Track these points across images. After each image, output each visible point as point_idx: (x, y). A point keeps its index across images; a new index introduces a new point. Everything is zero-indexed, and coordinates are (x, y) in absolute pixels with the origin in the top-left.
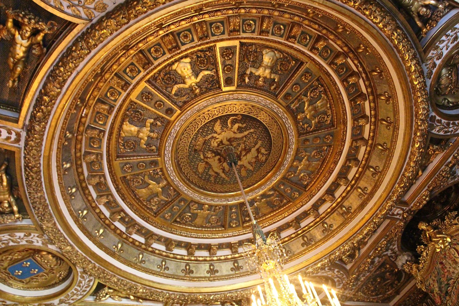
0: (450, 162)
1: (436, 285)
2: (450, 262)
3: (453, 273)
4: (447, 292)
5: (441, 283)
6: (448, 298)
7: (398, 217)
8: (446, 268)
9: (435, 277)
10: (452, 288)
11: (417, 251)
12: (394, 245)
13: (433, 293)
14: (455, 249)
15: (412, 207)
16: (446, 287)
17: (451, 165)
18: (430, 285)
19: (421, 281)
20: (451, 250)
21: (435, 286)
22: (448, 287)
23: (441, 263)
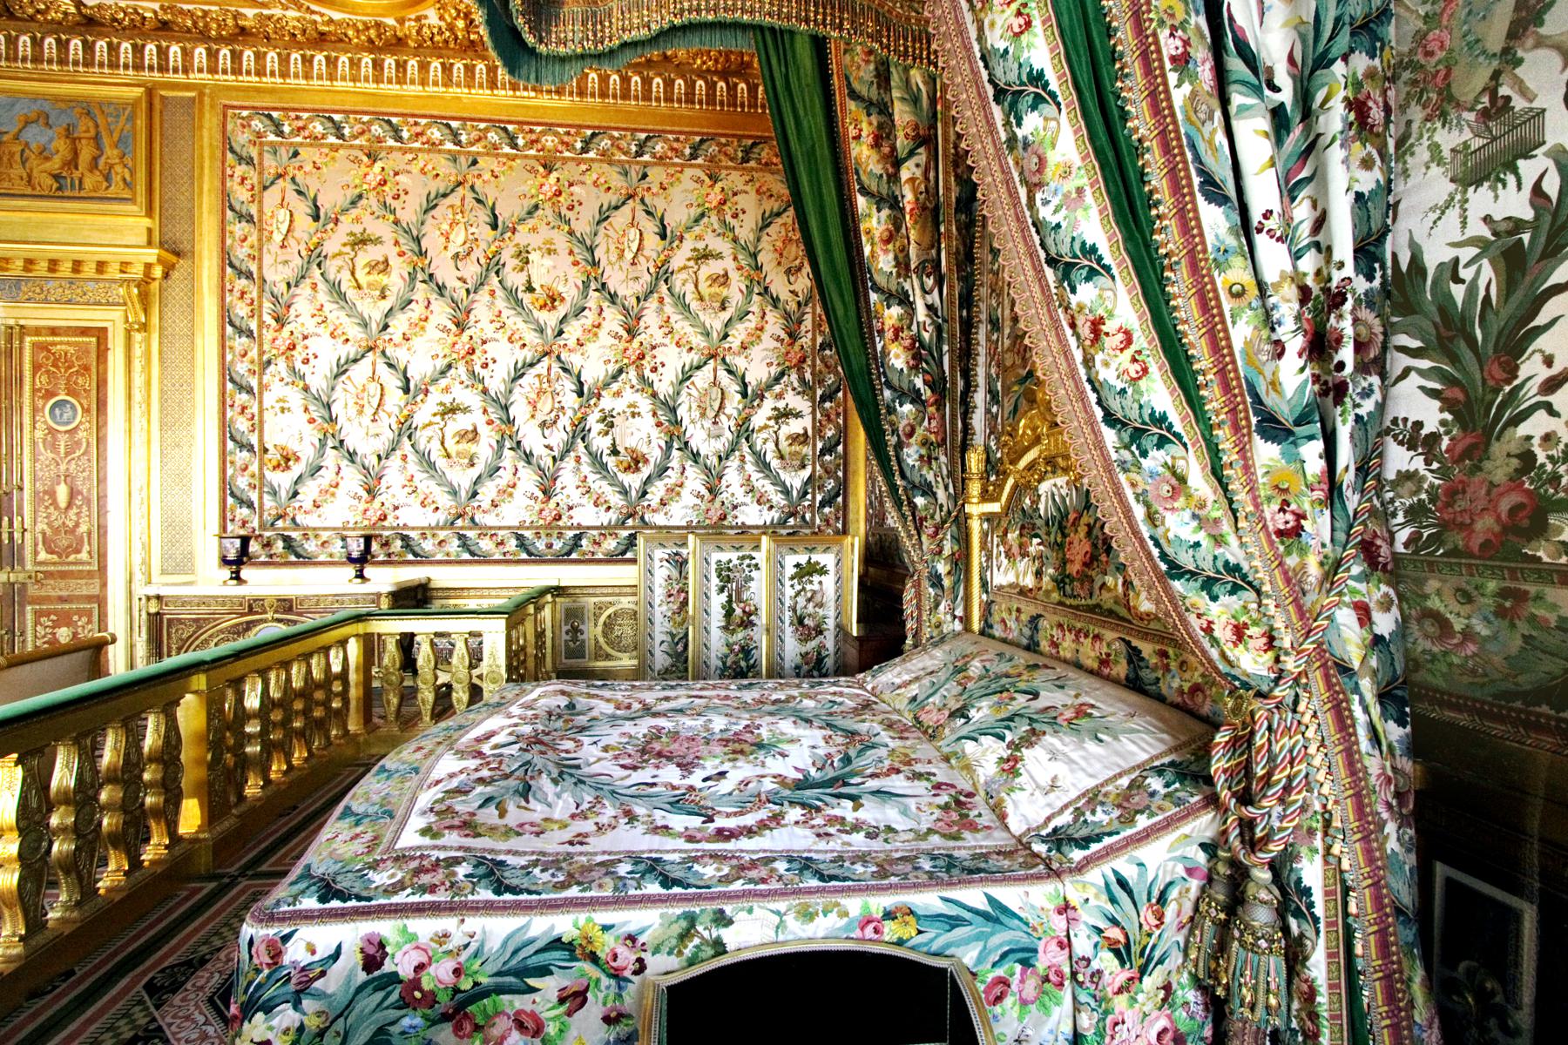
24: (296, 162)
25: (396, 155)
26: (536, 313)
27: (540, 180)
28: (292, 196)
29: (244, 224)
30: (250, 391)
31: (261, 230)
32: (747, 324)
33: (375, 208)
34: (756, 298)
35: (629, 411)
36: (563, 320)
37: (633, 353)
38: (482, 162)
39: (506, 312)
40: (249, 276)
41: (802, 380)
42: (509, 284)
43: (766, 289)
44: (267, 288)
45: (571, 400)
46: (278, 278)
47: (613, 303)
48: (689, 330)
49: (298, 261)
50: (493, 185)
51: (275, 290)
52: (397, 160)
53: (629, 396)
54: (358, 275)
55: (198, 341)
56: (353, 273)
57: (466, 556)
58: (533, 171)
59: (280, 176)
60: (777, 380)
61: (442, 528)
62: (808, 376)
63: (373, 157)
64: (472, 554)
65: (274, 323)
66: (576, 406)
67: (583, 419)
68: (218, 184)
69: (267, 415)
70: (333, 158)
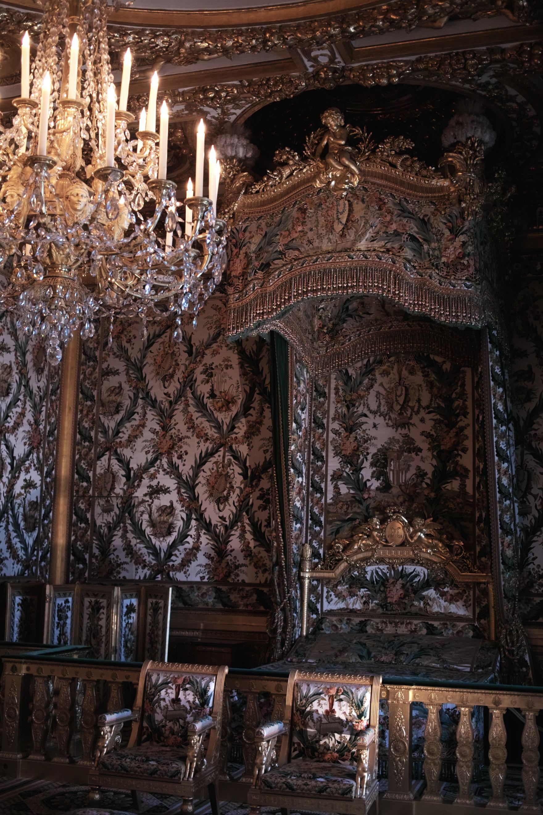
0: (503, 51)
1: (257, 239)
2: (322, 220)
3: (310, 242)
4: (268, 265)
5: (270, 243)
6: (260, 274)
7: (308, 64)
8: (304, 223)
9: (268, 225)
10: (284, 265)
11: (274, 155)
12: (237, 107)
13: (240, 249)
14: (350, 205)
15: (351, 70)
16: (275, 256)
17: (498, 57)
18: (245, 231)
19: (234, 214)
20: (341, 202)
21: (253, 240)
22: (280, 259)
23: (303, 211)
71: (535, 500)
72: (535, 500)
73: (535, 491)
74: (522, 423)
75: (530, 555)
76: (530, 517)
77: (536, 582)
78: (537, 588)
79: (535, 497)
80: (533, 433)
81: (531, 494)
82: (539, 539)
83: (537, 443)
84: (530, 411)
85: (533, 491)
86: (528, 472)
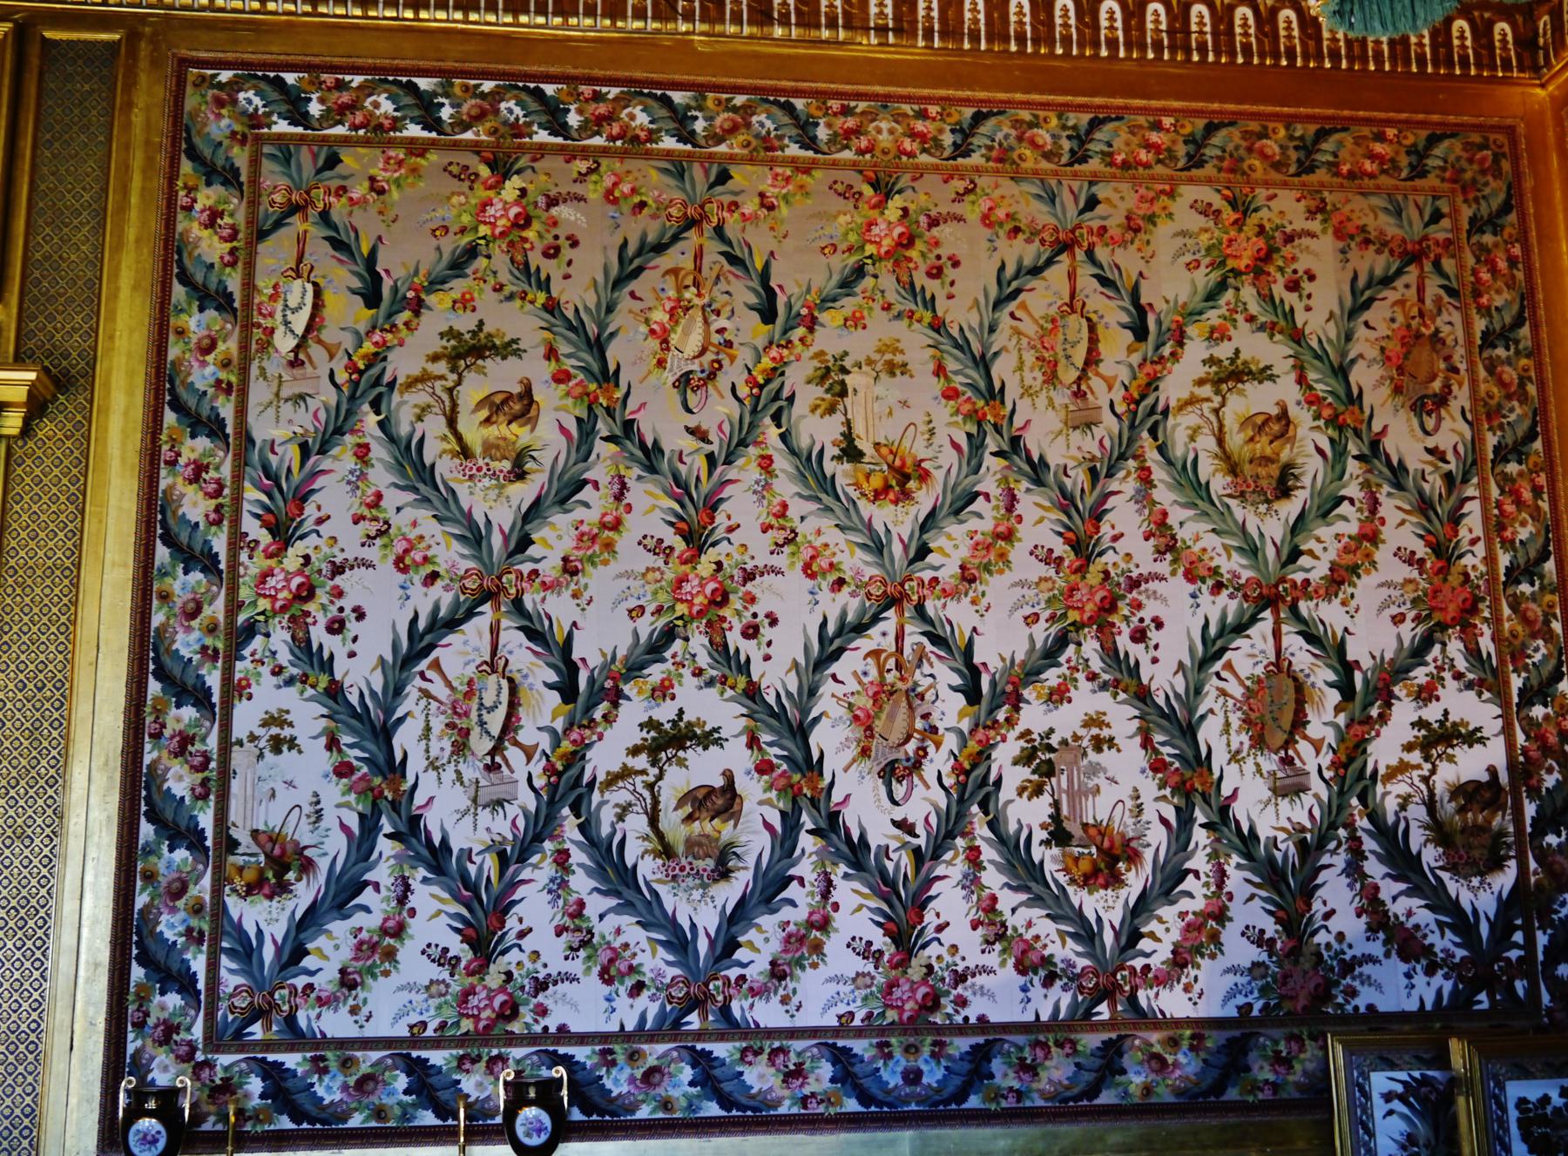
24: (723, 194)
25: (552, 163)
26: (866, 508)
27: (482, 193)
28: (320, 253)
29: (211, 314)
30: (201, 698)
31: (248, 327)
32: (973, 524)
33: (504, 277)
34: (992, 463)
35: (1087, 734)
36: (929, 523)
37: (698, 590)
38: (739, 175)
39: (393, 498)
40: (215, 428)
41: (1473, 652)
42: (803, 442)
43: (1015, 441)
44: (255, 457)
45: (950, 710)
46: (280, 433)
47: (652, 469)
48: (833, 537)
49: (329, 396)
50: (764, 226)
51: (274, 460)
52: (557, 174)
53: (1086, 699)
54: (461, 428)
55: (88, 577)
56: (452, 422)
57: (712, 1109)
58: (466, 176)
59: (293, 209)
60: (1051, 655)
61: (652, 1037)
62: (1486, 644)
63: (502, 168)
64: (725, 1102)
65: (265, 537)
66: (965, 725)
67: (983, 755)
68: (155, 225)
69: (238, 758)
70: (414, 170)
71: (529, 759)
72: (529, 759)
73: (527, 735)
74: (497, 541)
75: (511, 923)
76: (512, 810)
77: (527, 1003)
78: (529, 1019)
79: (529, 753)
80: (526, 568)
81: (516, 744)
82: (537, 875)
83: (538, 598)
84: (524, 509)
85: (522, 737)
86: (511, 680)
